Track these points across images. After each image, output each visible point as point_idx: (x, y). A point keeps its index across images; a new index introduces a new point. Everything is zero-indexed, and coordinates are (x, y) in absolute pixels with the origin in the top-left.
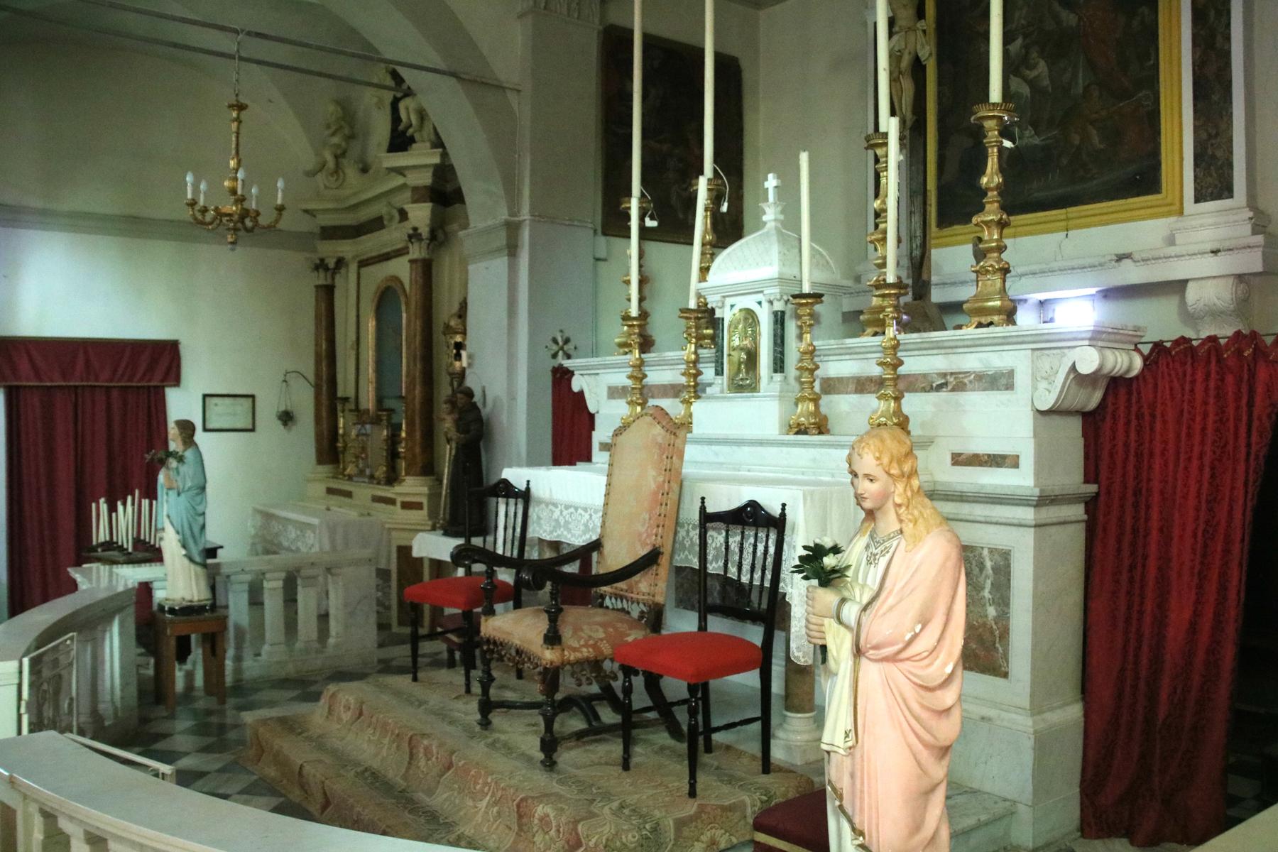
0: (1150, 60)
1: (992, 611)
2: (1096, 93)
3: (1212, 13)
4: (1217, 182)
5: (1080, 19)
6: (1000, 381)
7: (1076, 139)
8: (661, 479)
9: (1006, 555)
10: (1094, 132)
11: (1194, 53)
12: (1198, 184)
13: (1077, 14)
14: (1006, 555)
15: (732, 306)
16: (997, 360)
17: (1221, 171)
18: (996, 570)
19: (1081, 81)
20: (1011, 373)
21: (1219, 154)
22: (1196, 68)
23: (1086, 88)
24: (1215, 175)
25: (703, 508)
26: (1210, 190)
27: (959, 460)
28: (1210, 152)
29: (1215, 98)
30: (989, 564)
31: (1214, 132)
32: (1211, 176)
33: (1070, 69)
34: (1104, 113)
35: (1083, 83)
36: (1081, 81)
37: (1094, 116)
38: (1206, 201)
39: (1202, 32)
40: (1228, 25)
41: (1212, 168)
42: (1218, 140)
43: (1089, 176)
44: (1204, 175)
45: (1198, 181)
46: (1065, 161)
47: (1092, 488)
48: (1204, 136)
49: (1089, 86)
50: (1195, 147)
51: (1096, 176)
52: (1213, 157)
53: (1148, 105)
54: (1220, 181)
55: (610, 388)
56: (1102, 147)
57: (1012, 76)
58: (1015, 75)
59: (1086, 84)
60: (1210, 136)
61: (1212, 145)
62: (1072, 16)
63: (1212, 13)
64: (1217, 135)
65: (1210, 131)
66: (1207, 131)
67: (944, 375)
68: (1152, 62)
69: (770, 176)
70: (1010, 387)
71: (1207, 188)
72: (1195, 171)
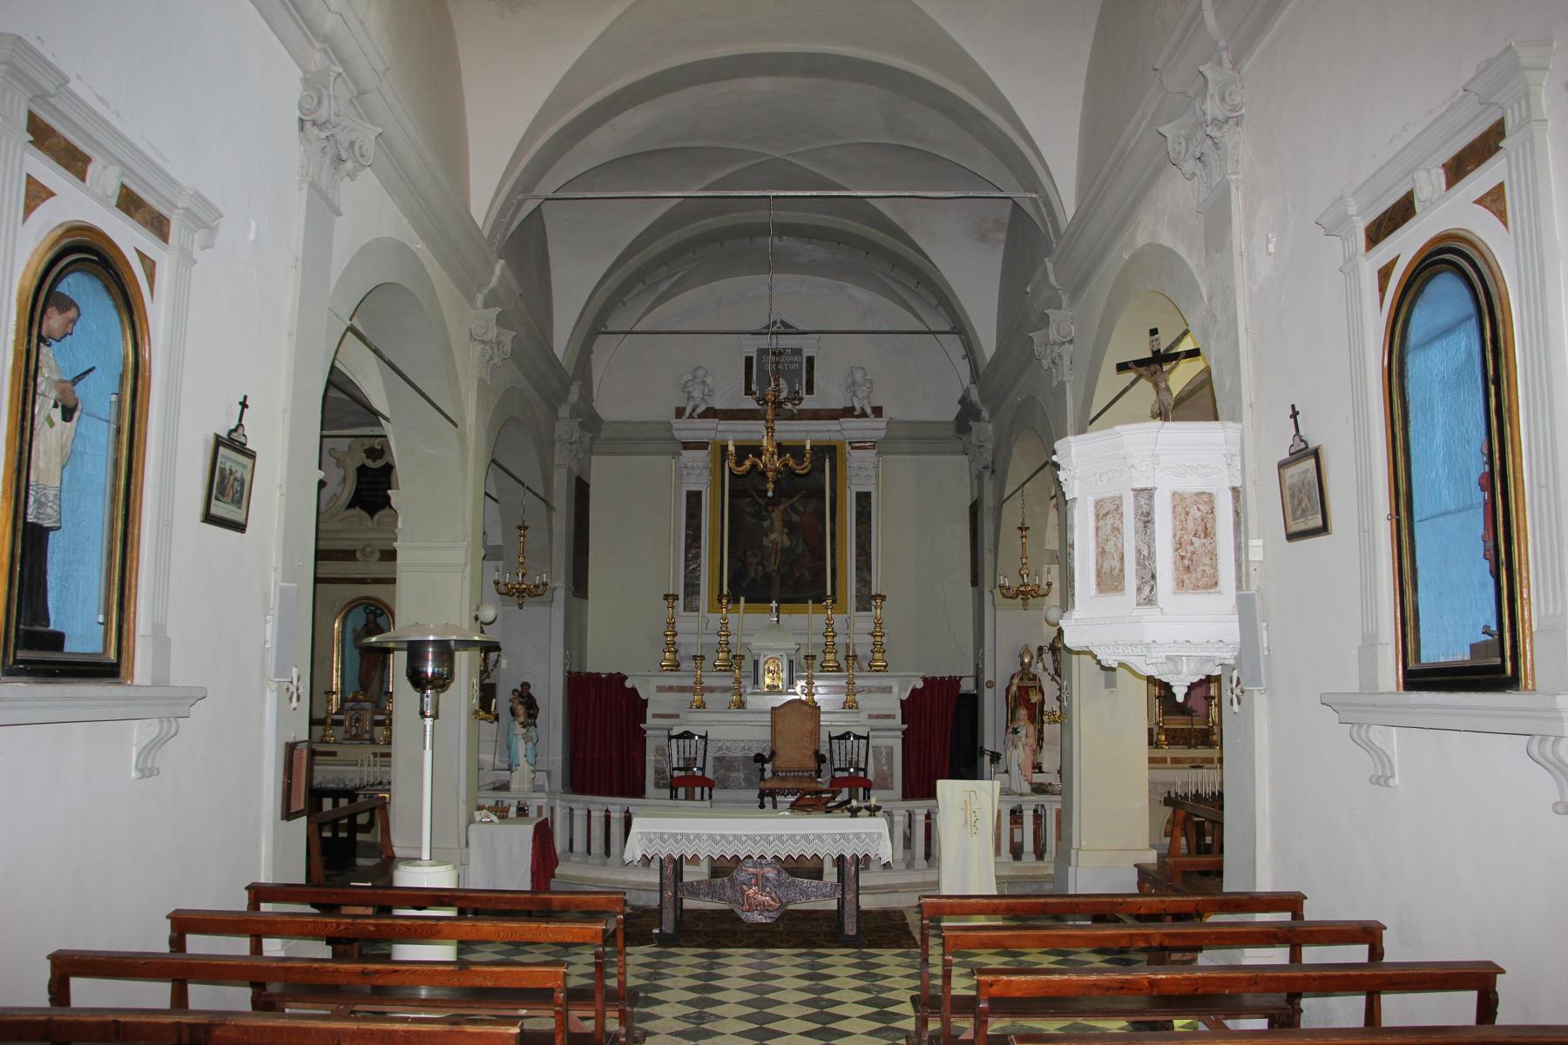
1: (885, 768)
2: (808, 554)
6: (889, 690)
7: (798, 574)
8: (814, 725)
9: (891, 748)
14: (891, 748)
15: (782, 656)
16: (885, 683)
18: (887, 753)
20: (891, 687)
23: (803, 551)
25: (830, 735)
27: (871, 717)
30: (884, 752)
47: (906, 726)
55: (658, 687)
62: (796, 517)
67: (863, 687)
69: (774, 602)
70: (890, 692)
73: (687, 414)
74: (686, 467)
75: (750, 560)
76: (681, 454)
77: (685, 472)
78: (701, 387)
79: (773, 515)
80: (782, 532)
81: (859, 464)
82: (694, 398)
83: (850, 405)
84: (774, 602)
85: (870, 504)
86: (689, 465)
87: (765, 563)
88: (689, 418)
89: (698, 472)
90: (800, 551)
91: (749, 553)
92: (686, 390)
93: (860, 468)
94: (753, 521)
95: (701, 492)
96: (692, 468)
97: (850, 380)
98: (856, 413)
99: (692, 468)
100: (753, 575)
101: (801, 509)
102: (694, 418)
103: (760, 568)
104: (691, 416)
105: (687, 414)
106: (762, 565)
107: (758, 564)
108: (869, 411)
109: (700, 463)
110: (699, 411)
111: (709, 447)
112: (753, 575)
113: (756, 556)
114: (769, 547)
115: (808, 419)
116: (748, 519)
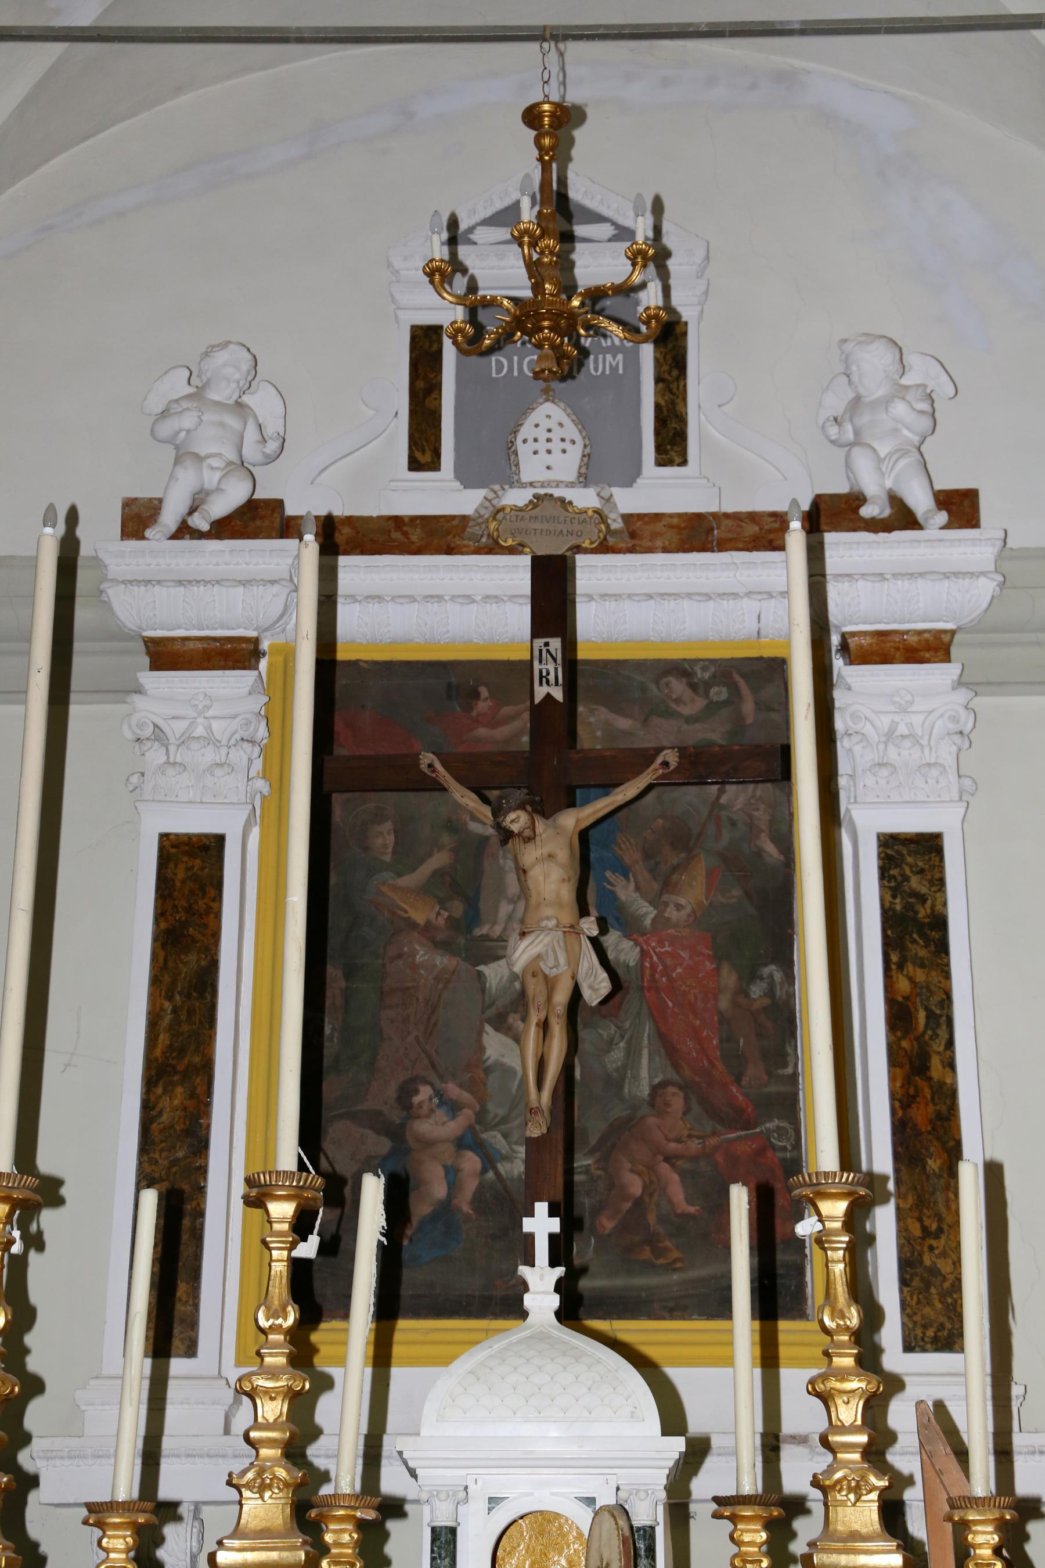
0: (785, 1065)
2: (677, 1101)
3: (922, 1016)
4: (942, 1319)
5: (644, 953)
7: (635, 1186)
10: (676, 1177)
11: (892, 1079)
12: (909, 1316)
13: (637, 943)
17: (949, 1300)
19: (644, 1073)
21: (945, 1266)
22: (897, 1104)
23: (655, 1089)
24: (939, 1306)
26: (930, 1333)
28: (927, 1261)
29: (933, 1165)
31: (934, 1227)
32: (929, 1304)
33: (622, 1044)
34: (694, 1145)
35: (651, 1078)
36: (644, 1073)
37: (673, 1146)
38: (924, 1350)
39: (905, 1044)
40: (950, 1043)
41: (933, 1290)
42: (943, 1241)
43: (661, 1261)
44: (919, 1302)
45: (909, 1310)
46: (607, 1224)
48: (916, 1230)
49: (664, 1084)
50: (900, 1248)
51: (679, 1265)
52: (934, 1271)
53: (784, 1149)
54: (949, 1318)
56: (692, 1209)
57: (488, 1028)
58: (497, 1029)
59: (657, 1081)
60: (926, 1232)
61: (931, 1248)
62: (627, 944)
63: (922, 1016)
64: (940, 1230)
65: (927, 1222)
66: (920, 1220)
68: (790, 1070)
69: (541, 1208)
71: (925, 1327)
72: (901, 1291)
73: (170, 517)
74: (159, 735)
75: (424, 1127)
76: (139, 690)
77: (155, 756)
78: (232, 422)
79: (530, 855)
80: (574, 930)
81: (885, 722)
82: (199, 459)
83: (841, 488)
84: (541, 1208)
85: (940, 883)
86: (175, 729)
87: (495, 1139)
88: (177, 535)
89: (209, 756)
90: (645, 1091)
91: (425, 1093)
92: (166, 429)
93: (890, 736)
94: (442, 961)
95: (219, 841)
96: (185, 740)
97: (836, 402)
98: (867, 511)
99: (185, 740)
100: (439, 1190)
101: (647, 912)
102: (198, 535)
103: (471, 1162)
104: (184, 531)
105: (170, 517)
106: (480, 1148)
107: (461, 1144)
108: (920, 501)
109: (216, 725)
110: (221, 506)
111: (263, 664)
112: (439, 1190)
113: (454, 1108)
114: (507, 1072)
115: (666, 550)
116: (422, 955)
